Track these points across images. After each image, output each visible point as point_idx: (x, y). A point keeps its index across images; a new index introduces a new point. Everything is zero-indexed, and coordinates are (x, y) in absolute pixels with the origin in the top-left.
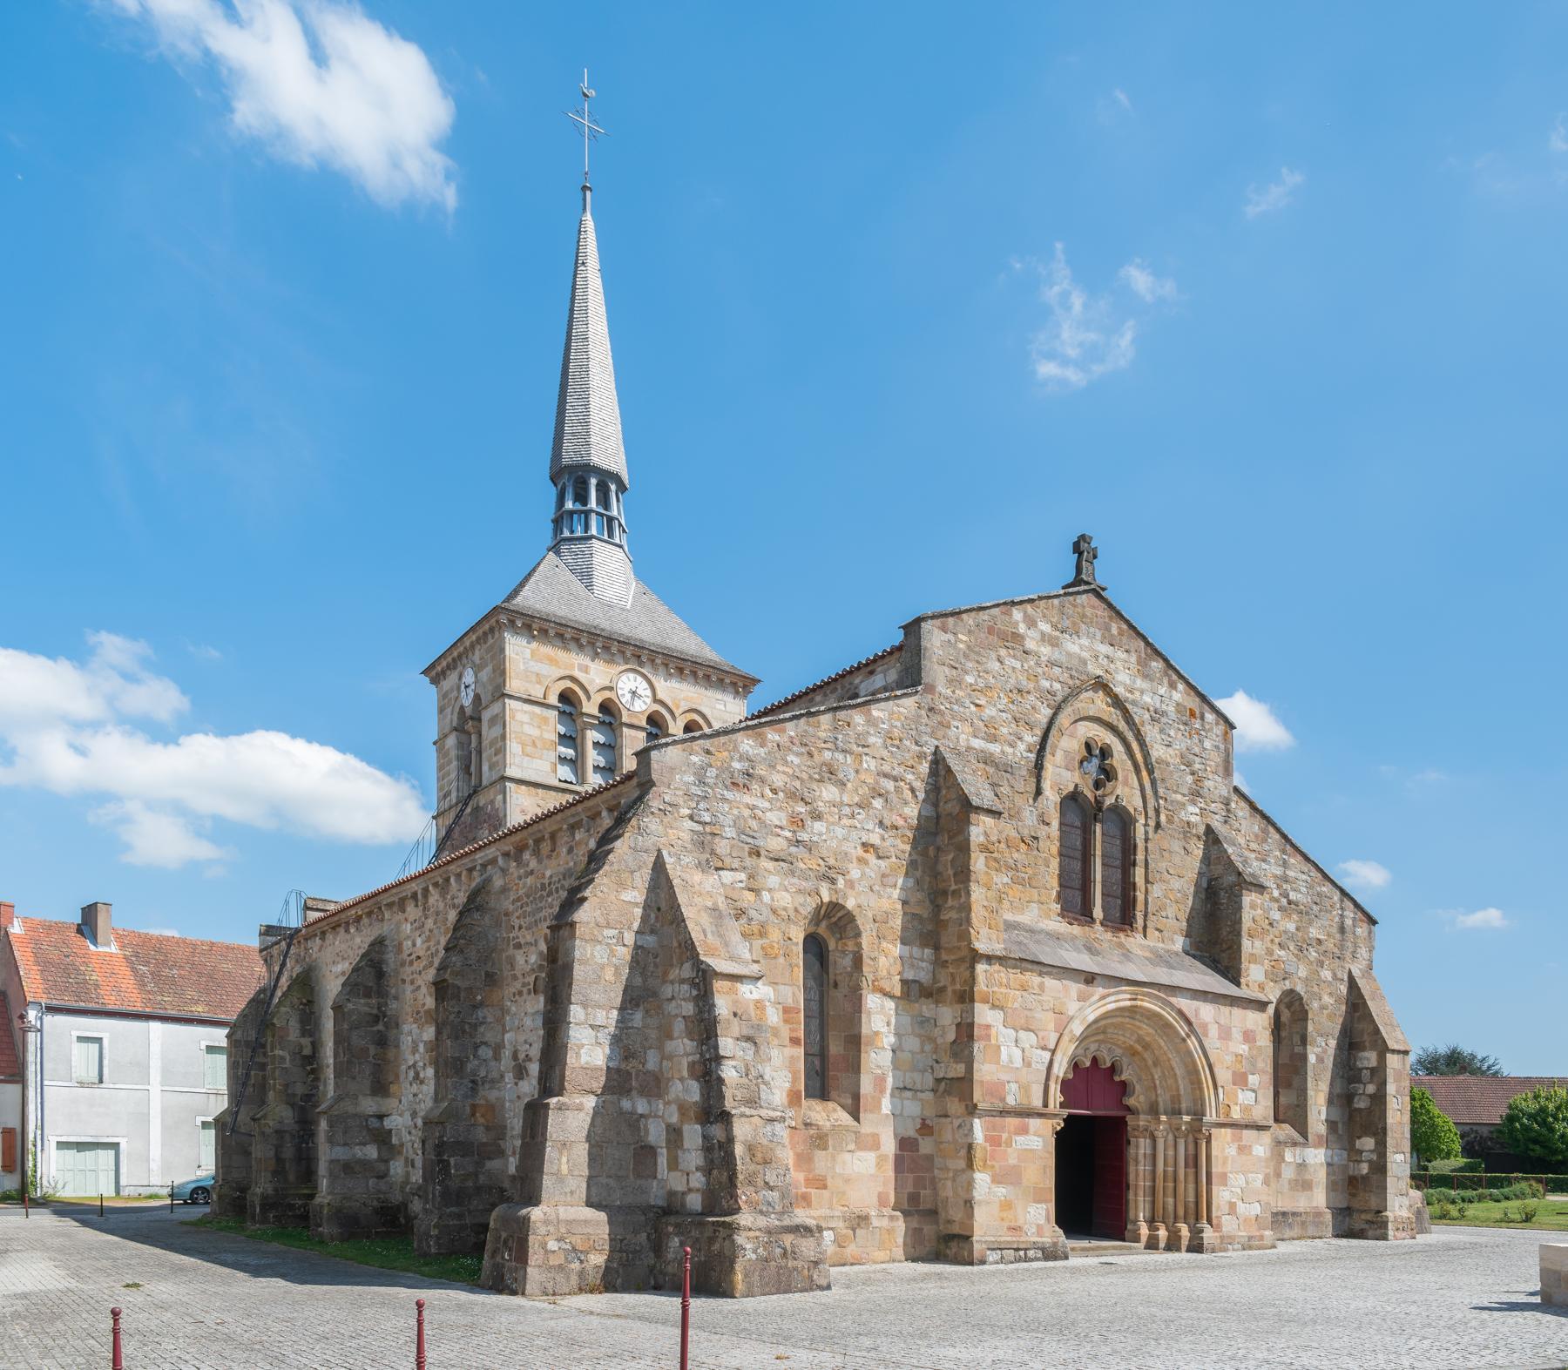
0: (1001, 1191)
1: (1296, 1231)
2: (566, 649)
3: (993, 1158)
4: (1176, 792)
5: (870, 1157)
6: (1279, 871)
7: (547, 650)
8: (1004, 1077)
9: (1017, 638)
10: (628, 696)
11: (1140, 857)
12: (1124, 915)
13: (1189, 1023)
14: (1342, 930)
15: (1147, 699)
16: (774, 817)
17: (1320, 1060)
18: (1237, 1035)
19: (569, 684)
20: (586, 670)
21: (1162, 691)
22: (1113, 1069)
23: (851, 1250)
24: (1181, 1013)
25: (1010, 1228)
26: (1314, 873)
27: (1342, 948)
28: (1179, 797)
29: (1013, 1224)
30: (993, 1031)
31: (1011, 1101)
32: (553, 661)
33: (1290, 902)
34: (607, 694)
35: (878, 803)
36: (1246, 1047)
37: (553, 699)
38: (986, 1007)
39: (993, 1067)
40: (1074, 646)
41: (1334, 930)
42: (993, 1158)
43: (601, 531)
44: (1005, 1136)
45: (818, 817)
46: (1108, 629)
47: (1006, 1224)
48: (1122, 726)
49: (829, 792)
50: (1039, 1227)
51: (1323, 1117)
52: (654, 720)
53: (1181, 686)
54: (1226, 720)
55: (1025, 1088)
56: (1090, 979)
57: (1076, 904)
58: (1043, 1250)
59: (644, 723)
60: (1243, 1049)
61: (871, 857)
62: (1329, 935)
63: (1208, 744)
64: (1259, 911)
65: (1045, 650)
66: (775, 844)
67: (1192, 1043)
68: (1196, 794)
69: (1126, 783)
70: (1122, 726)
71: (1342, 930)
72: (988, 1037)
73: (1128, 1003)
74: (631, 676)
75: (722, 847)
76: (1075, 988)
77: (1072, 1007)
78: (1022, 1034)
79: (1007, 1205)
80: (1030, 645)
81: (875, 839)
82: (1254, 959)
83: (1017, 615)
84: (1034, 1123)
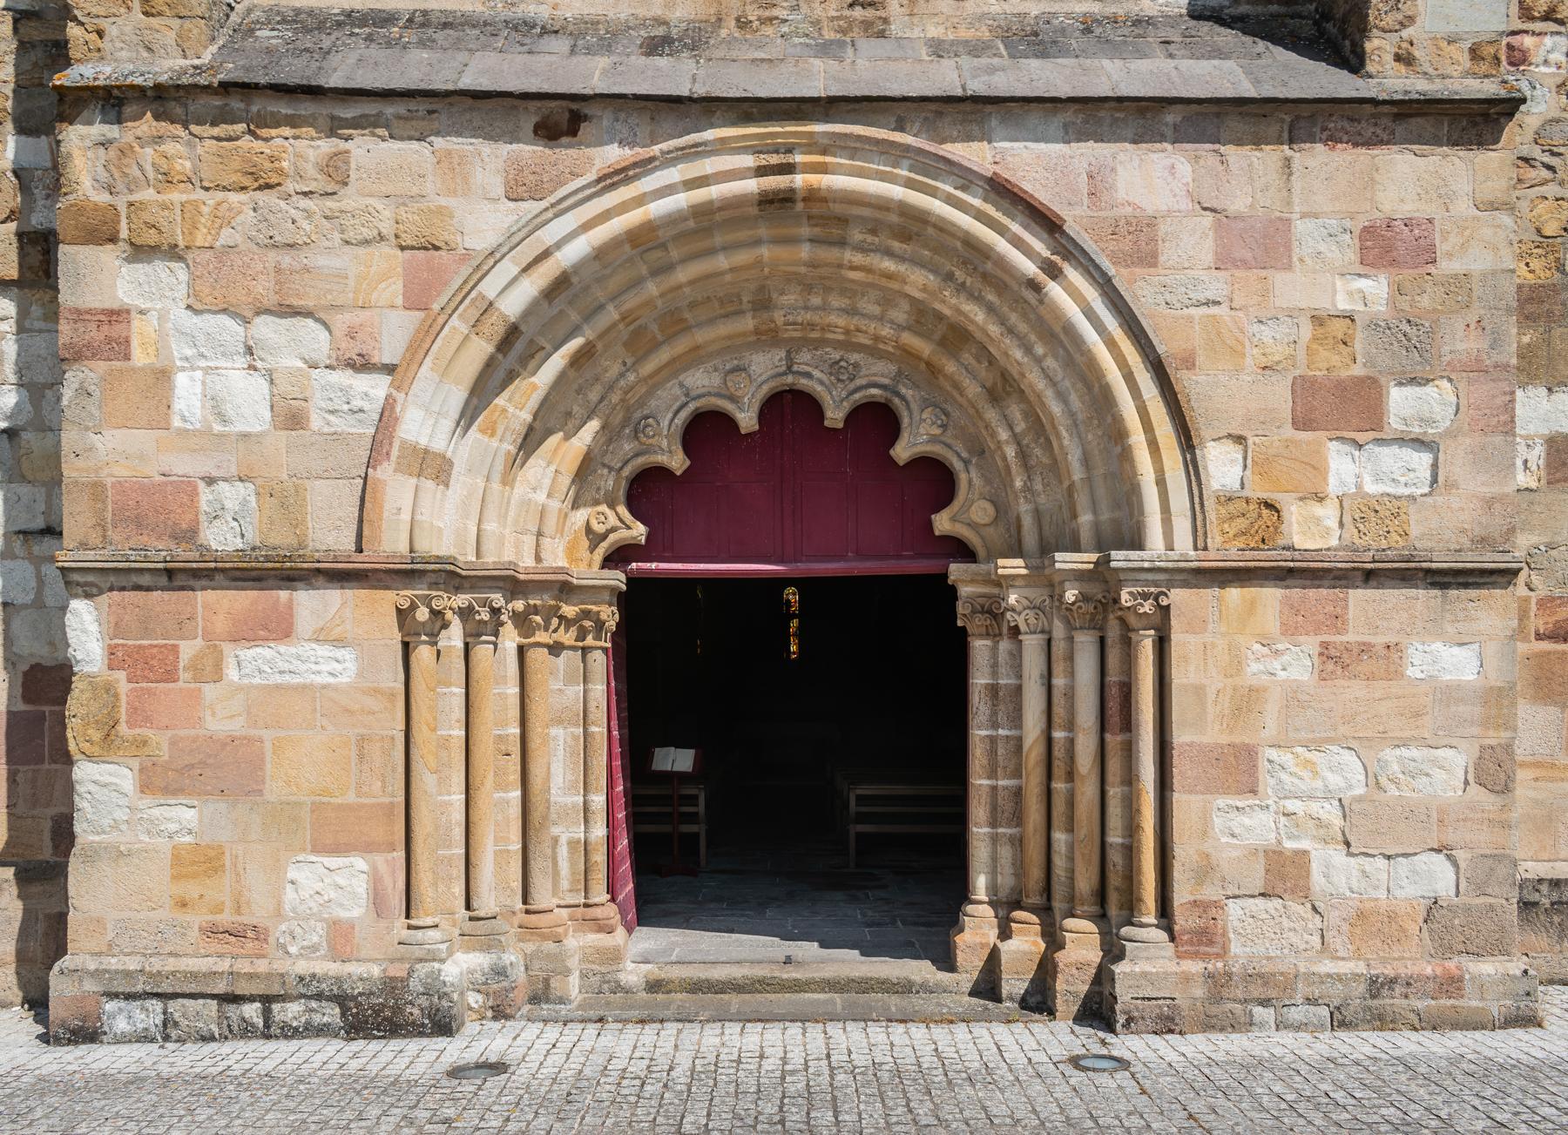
3: (139, 715)
8: (185, 465)
13: (1048, 223)
18: (1322, 241)
24: (1002, 191)
25: (212, 931)
29: (226, 918)
30: (141, 332)
31: (222, 539)
36: (1376, 289)
38: (108, 256)
39: (140, 439)
42: (139, 715)
44: (188, 649)
47: (197, 919)
50: (340, 937)
58: (341, 1000)
67: (1072, 298)
72: (121, 348)
73: (751, 185)
76: (490, 159)
77: (483, 220)
78: (267, 329)
79: (199, 862)
84: (309, 604)
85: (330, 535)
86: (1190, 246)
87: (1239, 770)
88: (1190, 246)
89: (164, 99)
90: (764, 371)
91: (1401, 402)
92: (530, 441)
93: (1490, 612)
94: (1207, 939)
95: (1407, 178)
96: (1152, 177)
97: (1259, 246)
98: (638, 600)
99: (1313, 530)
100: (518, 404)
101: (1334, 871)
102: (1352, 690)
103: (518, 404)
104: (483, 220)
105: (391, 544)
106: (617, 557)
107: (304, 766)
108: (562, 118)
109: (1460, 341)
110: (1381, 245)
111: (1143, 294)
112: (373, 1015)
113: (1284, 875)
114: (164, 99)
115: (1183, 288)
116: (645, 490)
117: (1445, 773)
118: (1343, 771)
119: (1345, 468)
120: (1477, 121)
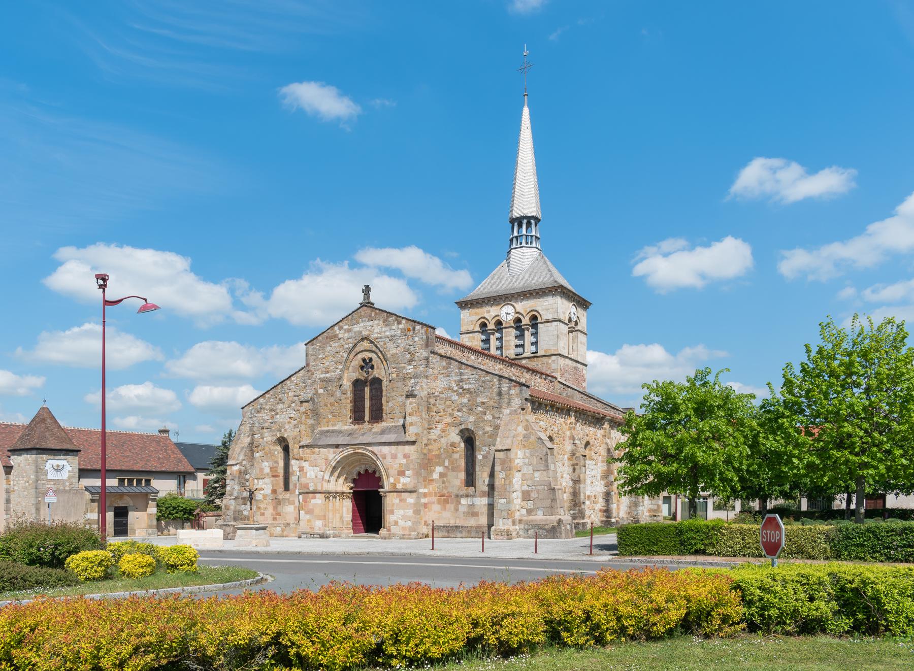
0: (308, 516)
1: (464, 534)
2: (482, 307)
5: (292, 507)
6: (458, 378)
7: (475, 310)
9: (336, 336)
11: (384, 393)
12: (377, 416)
14: (500, 394)
15: (388, 333)
16: (267, 417)
17: (485, 457)
18: (400, 456)
19: (482, 320)
20: (488, 312)
21: (394, 327)
22: (374, 472)
23: (285, 533)
26: (480, 373)
27: (500, 403)
31: (311, 489)
32: (476, 314)
34: (497, 318)
35: (293, 405)
36: (404, 461)
37: (478, 328)
40: (356, 328)
41: (494, 395)
43: (527, 243)
45: (277, 414)
46: (370, 316)
48: (374, 348)
49: (280, 406)
51: (487, 483)
52: (518, 320)
53: (404, 321)
54: (426, 326)
55: (316, 485)
56: (337, 446)
57: (358, 417)
59: (512, 324)
60: (404, 461)
61: (292, 421)
62: (490, 399)
63: (416, 339)
65: (346, 335)
66: (267, 425)
68: (410, 361)
69: (378, 368)
70: (374, 348)
71: (500, 394)
75: (255, 429)
76: (332, 450)
77: (331, 456)
79: (309, 521)
80: (340, 336)
81: (292, 415)
82: (411, 424)
83: (336, 328)
84: (318, 495)
85: (319, 489)
86: (389, 457)
87: (392, 512)
88: (389, 457)
89: (307, 446)
90: (363, 467)
91: (407, 473)
92: (339, 477)
93: (414, 495)
94: (389, 530)
95: (408, 449)
96: (386, 450)
97: (394, 457)
98: (355, 493)
99: (399, 487)
100: (336, 474)
101: (400, 523)
102: (402, 504)
103: (336, 474)
104: (331, 456)
105: (324, 489)
106: (351, 488)
107: (317, 512)
108: (337, 446)
109: (412, 466)
110: (406, 456)
111: (385, 462)
112: (322, 536)
113: (396, 523)
114: (307, 446)
115: (388, 461)
116: (354, 481)
117: (410, 512)
118: (401, 512)
119: (402, 480)
120: (413, 443)
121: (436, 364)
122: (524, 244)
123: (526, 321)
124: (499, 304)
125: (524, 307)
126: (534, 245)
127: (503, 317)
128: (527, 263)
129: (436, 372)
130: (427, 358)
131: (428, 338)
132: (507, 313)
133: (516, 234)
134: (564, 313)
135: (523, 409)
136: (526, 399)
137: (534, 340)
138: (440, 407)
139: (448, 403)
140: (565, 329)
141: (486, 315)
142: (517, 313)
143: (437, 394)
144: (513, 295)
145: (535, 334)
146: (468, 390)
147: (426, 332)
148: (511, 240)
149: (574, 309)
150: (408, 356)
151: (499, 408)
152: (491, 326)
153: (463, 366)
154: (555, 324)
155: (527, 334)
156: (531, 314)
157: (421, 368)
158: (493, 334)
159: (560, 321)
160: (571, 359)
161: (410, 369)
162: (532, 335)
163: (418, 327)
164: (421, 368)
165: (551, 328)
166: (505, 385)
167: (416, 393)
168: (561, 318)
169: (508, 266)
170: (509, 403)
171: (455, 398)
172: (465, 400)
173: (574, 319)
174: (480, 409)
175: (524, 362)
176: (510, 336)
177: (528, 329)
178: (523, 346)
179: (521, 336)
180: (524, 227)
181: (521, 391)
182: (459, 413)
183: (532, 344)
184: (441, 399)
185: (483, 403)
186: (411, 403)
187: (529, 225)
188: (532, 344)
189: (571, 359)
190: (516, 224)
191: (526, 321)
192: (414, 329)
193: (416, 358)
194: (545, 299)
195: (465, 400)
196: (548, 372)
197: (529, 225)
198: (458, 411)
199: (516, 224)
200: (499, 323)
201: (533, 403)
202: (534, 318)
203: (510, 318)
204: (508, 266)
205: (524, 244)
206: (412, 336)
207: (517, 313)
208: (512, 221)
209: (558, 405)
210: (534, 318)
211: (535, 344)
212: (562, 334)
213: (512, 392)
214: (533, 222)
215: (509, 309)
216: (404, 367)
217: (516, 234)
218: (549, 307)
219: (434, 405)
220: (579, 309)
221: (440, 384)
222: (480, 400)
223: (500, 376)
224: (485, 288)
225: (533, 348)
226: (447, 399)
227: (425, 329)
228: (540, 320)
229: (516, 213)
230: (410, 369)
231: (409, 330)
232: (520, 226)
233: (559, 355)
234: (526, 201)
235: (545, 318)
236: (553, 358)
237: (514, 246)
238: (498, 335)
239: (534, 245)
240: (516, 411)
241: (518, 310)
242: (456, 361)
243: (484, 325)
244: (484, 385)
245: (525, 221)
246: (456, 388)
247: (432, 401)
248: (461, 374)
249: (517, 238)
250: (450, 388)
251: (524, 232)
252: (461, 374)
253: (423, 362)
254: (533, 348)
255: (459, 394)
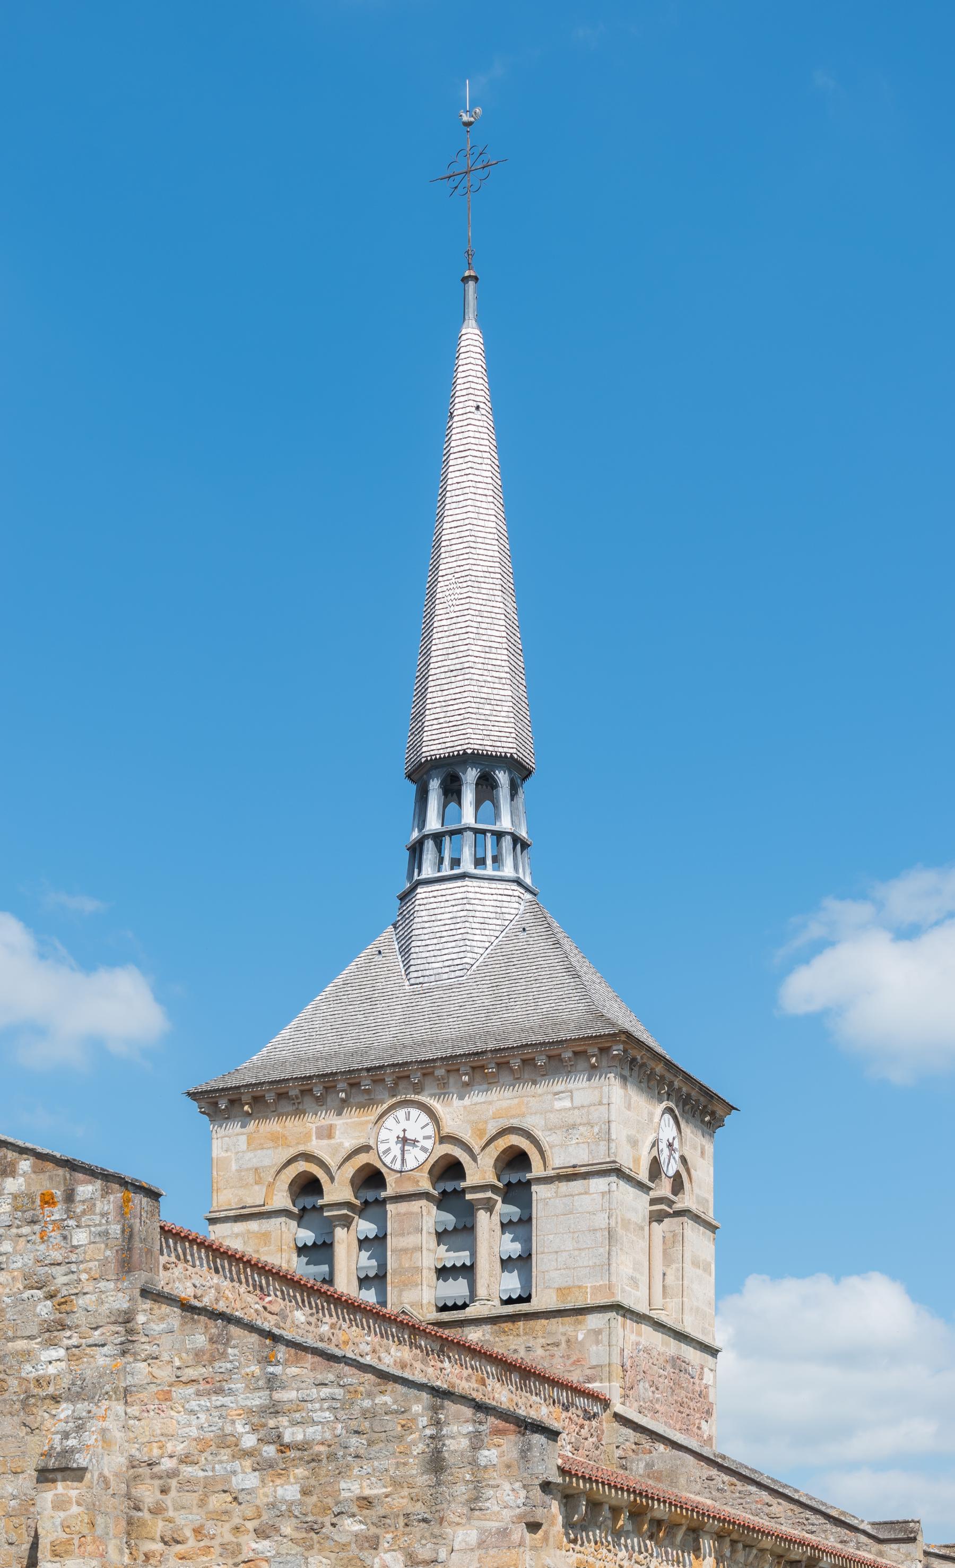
2: (299, 1112)
4: (13, 1339)
6: (257, 1400)
7: (272, 1126)
10: (396, 1150)
14: (436, 1463)
26: (352, 1377)
27: (435, 1501)
28: (21, 1344)
32: (277, 1140)
33: (284, 1448)
34: (362, 1159)
37: (282, 1200)
41: (414, 1470)
43: (480, 862)
52: (450, 1169)
53: (25, 1165)
54: (123, 1183)
59: (425, 1185)
62: (397, 1483)
63: (80, 1237)
64: (75, 1509)
68: (53, 1330)
71: (436, 1463)
74: (401, 1113)
121: (166, 1341)
122: (467, 865)
123: (480, 1171)
124: (369, 1102)
125: (475, 1115)
126: (508, 870)
127: (389, 1156)
128: (481, 942)
129: (164, 1373)
130: (126, 1319)
131: (129, 1235)
132: (403, 1138)
133: (433, 824)
134: (634, 1143)
135: (534, 1527)
136: (546, 1487)
137: (515, 1249)
138: (181, 1518)
139: (217, 1501)
140: (635, 1204)
141: (316, 1147)
142: (445, 1139)
143: (168, 1464)
144: (427, 1068)
145: (521, 1226)
146: (301, 1447)
147: (123, 1211)
148: (416, 850)
149: (668, 1131)
150: (45, 1309)
151: (433, 1520)
152: (338, 1191)
153: (282, 1352)
154: (598, 1184)
155: (486, 1223)
156: (503, 1143)
157: (102, 1359)
158: (347, 1222)
159: (618, 1172)
160: (659, 1326)
161: (51, 1362)
162: (505, 1226)
163: (87, 1189)
164: (102, 1359)
165: (584, 1203)
166: (459, 1428)
167: (81, 1460)
168: (625, 1161)
169: (405, 951)
170: (474, 1504)
171: (246, 1479)
172: (289, 1491)
173: (671, 1167)
174: (352, 1526)
175: (474, 1335)
176: (416, 1232)
177: (489, 1206)
178: (468, 1271)
179: (461, 1232)
180: (468, 796)
181: (524, 1453)
182: (264, 1546)
183: (507, 1263)
184: (187, 1485)
185: (366, 1502)
186: (60, 1504)
187: (486, 785)
188: (507, 1263)
189: (659, 1326)
190: (434, 785)
191: (480, 1171)
192: (70, 1197)
193: (79, 1318)
194: (560, 1085)
195: (289, 1491)
196: (575, 1378)
197: (486, 785)
198: (261, 1533)
199: (434, 785)
200: (371, 1178)
201: (568, 1499)
202: (516, 1160)
203: (415, 1157)
204: (405, 951)
205: (467, 865)
206: (60, 1225)
207: (445, 1139)
208: (420, 773)
209: (660, 1511)
210: (516, 1160)
211: (521, 1263)
212: (626, 1223)
213: (488, 1455)
214: (502, 777)
215: (414, 1123)
216: (27, 1355)
217: (433, 824)
218: (575, 1117)
219: (156, 1511)
220: (687, 1129)
221: (181, 1424)
222: (351, 1488)
223: (435, 1392)
224: (303, 1039)
225: (511, 1283)
226: (209, 1487)
227: (117, 1195)
228: (537, 1170)
229: (437, 742)
230: (51, 1362)
231: (48, 1200)
232: (452, 791)
233: (617, 1308)
234: (475, 691)
235: (559, 1159)
236: (594, 1321)
237: (428, 871)
238: (366, 1227)
239: (508, 870)
240: (504, 1533)
241: (451, 1125)
242: (251, 1328)
243: (308, 1186)
244: (369, 1428)
245: (471, 776)
246: (249, 1441)
247: (148, 1493)
248: (272, 1383)
249: (438, 838)
250: (226, 1441)
251: (468, 817)
252: (272, 1383)
253: (111, 1334)
254: (511, 1283)
255: (263, 1467)
